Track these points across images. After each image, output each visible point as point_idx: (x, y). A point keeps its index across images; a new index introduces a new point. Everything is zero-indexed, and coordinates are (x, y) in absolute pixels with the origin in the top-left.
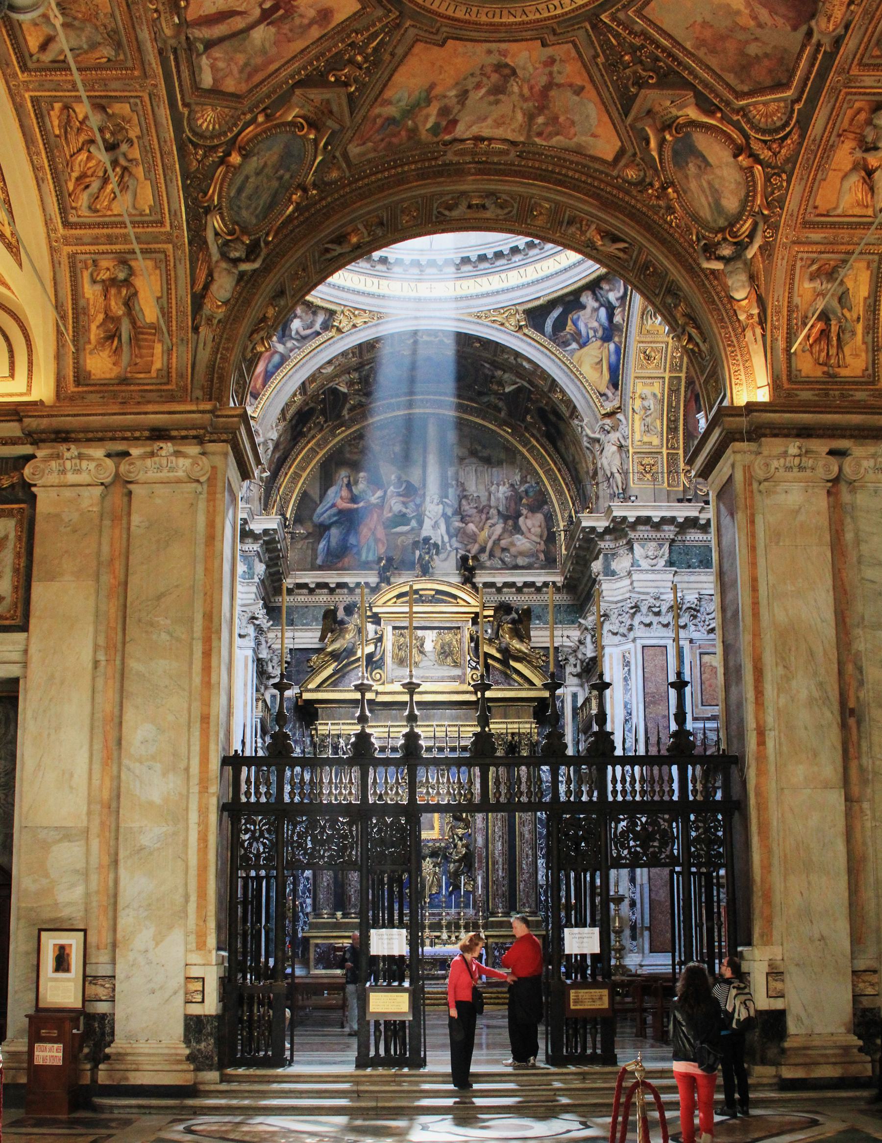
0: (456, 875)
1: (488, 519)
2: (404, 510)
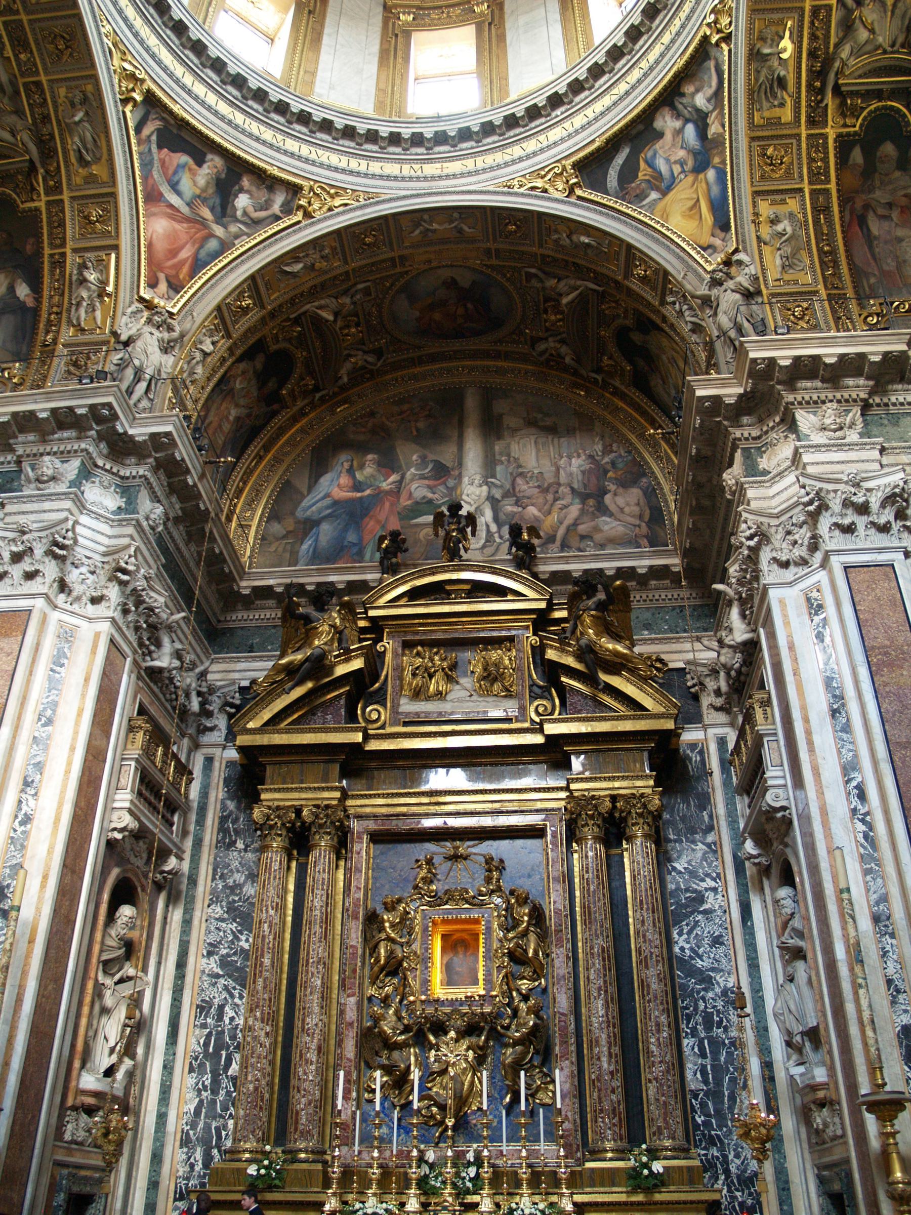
0: (517, 1066)
1: (556, 500)
2: (430, 495)
